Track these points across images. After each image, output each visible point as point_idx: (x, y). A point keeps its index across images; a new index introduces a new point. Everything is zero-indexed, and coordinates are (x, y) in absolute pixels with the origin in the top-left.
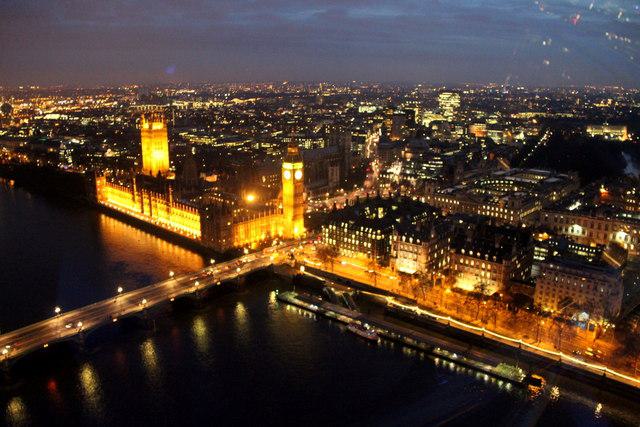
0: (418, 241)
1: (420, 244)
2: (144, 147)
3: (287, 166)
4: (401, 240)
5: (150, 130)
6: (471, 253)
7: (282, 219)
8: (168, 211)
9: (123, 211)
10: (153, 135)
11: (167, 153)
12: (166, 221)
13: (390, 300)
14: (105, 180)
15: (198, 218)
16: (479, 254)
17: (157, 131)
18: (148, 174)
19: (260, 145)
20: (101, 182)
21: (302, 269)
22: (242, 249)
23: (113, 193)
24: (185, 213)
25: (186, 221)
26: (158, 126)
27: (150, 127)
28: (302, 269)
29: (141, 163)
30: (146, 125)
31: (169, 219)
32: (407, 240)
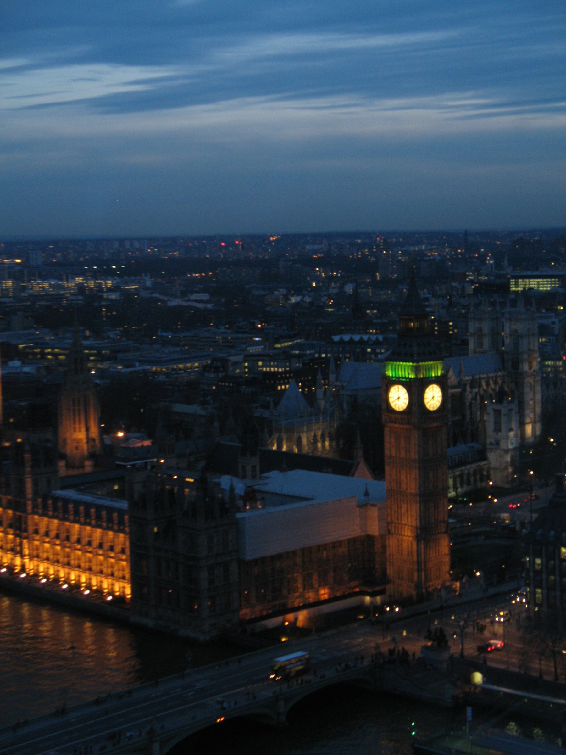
15: (122, 539)
21: (478, 677)
31: (17, 551)
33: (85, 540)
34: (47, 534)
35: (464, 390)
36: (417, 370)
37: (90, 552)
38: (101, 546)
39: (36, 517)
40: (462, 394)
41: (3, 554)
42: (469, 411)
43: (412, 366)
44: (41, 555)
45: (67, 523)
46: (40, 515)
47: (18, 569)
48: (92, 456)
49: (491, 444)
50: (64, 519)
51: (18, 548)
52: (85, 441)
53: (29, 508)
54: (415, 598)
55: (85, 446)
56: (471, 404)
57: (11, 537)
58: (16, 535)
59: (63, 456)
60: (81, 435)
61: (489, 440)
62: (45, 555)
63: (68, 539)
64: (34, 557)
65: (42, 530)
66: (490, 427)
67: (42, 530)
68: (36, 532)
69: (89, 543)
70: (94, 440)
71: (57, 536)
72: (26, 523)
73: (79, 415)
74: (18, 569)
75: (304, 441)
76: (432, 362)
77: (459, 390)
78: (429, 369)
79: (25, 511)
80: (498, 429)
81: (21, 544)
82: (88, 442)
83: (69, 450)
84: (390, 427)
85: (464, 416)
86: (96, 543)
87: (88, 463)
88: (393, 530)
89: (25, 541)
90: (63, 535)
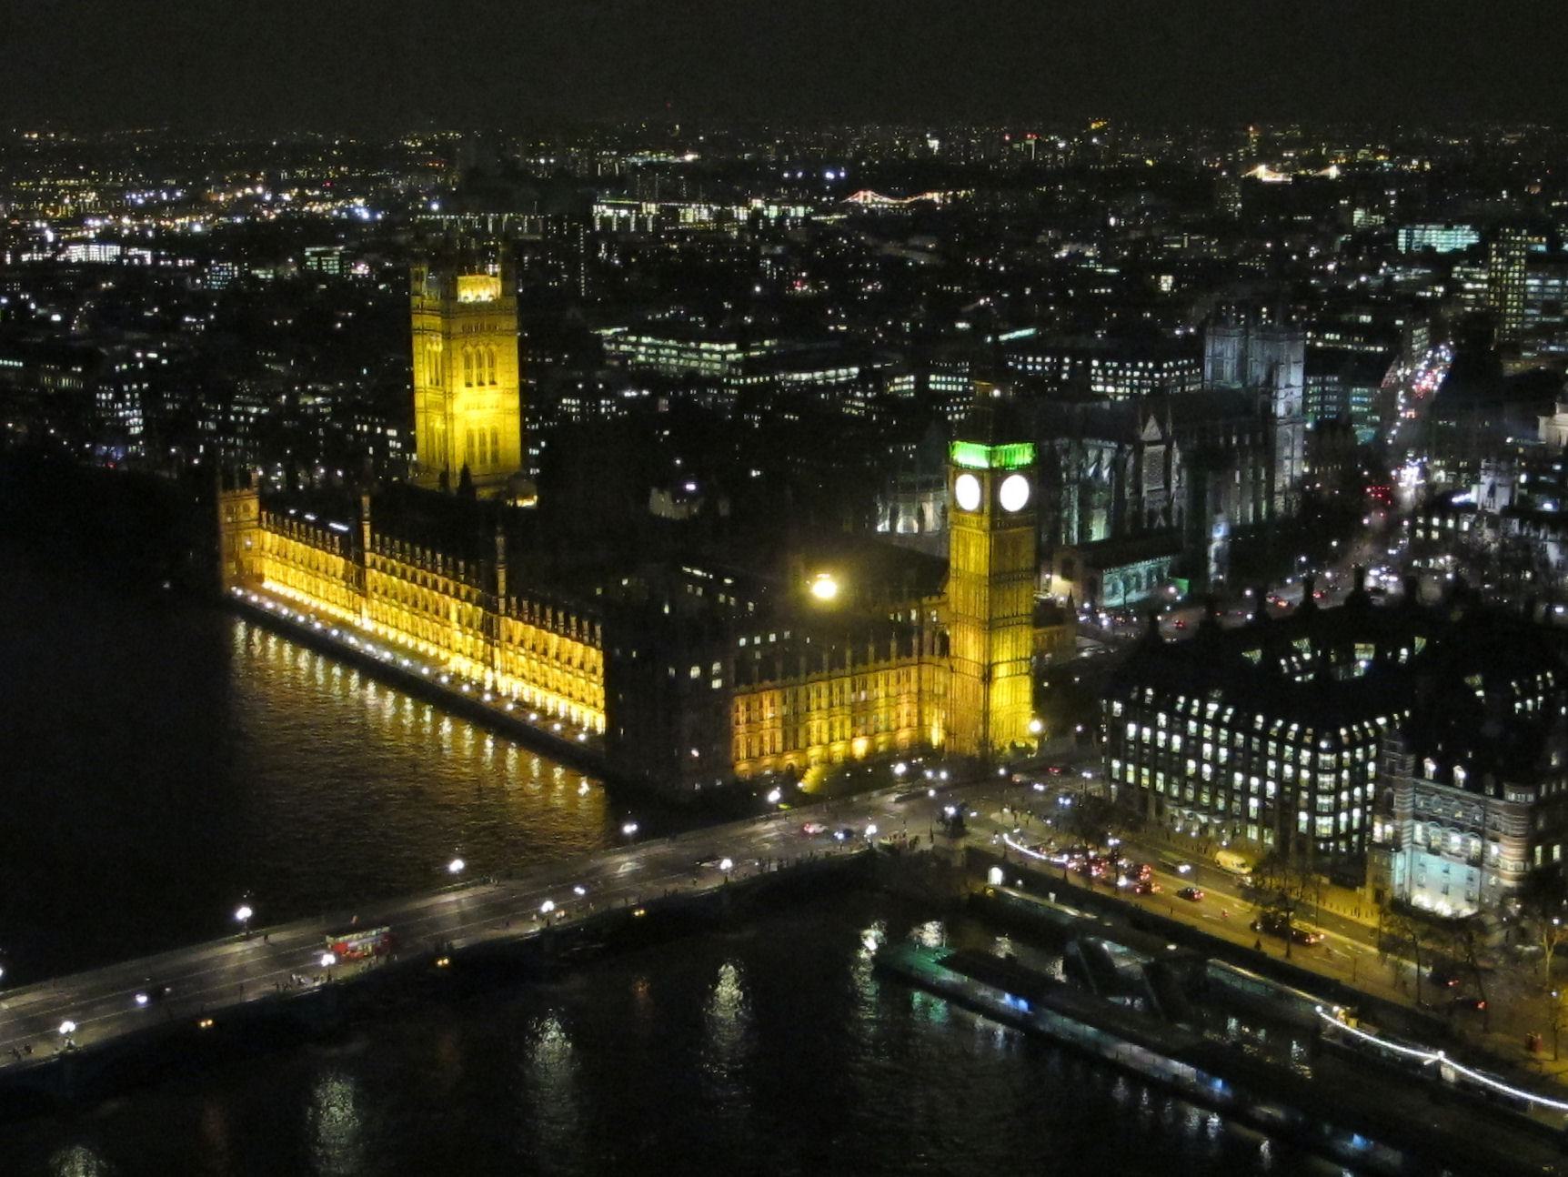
2: (423, 376)
3: (969, 454)
4: (1419, 771)
5: (450, 308)
7: (941, 677)
8: (489, 631)
10: (457, 328)
11: (514, 402)
12: (476, 671)
13: (1337, 1018)
14: (254, 505)
17: (478, 308)
18: (433, 484)
19: (921, 384)
21: (996, 876)
22: (762, 785)
23: (283, 556)
25: (555, 675)
28: (996, 876)
29: (410, 444)
32: (1445, 776)
33: (564, 657)
34: (522, 644)
35: (1169, 448)
36: (991, 456)
37: (570, 673)
38: (582, 666)
39: (510, 620)
40: (1168, 455)
41: (473, 665)
42: (1177, 478)
43: (986, 451)
44: (515, 670)
45: (544, 632)
46: (514, 619)
47: (488, 686)
50: (542, 627)
51: (489, 659)
53: (502, 606)
57: (481, 643)
58: (487, 641)
62: (519, 671)
63: (545, 653)
64: (507, 672)
65: (517, 639)
67: (517, 639)
68: (510, 640)
69: (569, 661)
71: (534, 648)
72: (498, 628)
74: (488, 686)
76: (1015, 445)
77: (1162, 448)
78: (1012, 454)
79: (495, 610)
81: (492, 655)
84: (958, 531)
86: (576, 662)
88: (956, 666)
89: (497, 651)
90: (540, 648)
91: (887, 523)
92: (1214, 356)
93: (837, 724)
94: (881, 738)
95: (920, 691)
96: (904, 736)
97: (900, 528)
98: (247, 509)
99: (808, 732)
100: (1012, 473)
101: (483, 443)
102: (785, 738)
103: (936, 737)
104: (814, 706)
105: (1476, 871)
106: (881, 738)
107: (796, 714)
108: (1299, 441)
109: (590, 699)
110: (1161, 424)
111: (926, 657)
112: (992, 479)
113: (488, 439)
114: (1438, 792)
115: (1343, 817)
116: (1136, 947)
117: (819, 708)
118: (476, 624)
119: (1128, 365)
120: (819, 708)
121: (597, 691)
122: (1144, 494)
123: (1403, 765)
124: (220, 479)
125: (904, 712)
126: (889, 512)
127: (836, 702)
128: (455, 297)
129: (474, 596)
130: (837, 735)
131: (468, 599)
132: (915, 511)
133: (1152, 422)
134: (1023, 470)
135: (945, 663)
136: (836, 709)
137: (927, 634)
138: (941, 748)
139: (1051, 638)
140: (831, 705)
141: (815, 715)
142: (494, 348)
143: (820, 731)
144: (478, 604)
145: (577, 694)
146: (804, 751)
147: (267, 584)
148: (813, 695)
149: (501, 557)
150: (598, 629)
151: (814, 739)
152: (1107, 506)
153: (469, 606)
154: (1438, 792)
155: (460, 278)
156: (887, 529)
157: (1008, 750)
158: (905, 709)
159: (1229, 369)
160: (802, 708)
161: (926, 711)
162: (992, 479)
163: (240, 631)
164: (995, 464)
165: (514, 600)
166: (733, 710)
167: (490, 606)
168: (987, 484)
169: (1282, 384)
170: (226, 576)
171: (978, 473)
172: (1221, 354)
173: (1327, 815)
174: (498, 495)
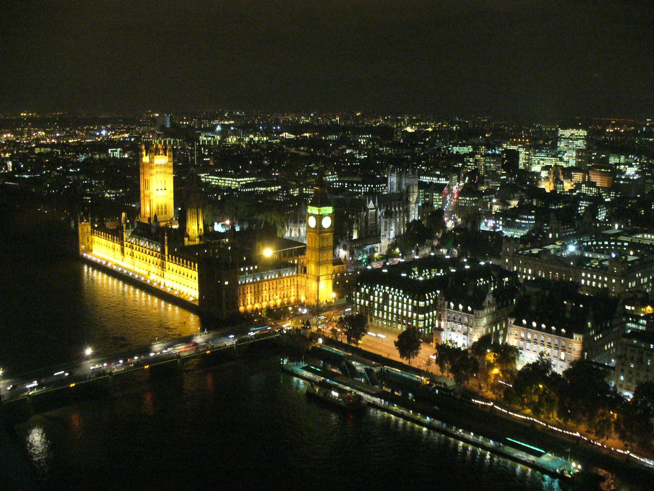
0: (470, 308)
1: (472, 313)
3: (312, 210)
4: (449, 306)
6: (534, 324)
7: (304, 280)
8: (163, 266)
9: (99, 261)
11: (172, 195)
12: (159, 279)
16: (543, 326)
18: (147, 222)
19: (301, 191)
20: (85, 227)
21: (320, 341)
24: (183, 269)
25: (184, 280)
26: (162, 160)
27: (151, 162)
28: (320, 341)
30: (146, 159)
32: (456, 308)
35: (377, 211)
36: (319, 210)
40: (376, 212)
47: (162, 284)
48: (200, 237)
49: (383, 236)
52: (197, 230)
54: (315, 306)
55: (197, 232)
56: (380, 217)
57: (160, 270)
59: (188, 236)
60: (195, 227)
61: (382, 234)
66: (383, 228)
70: (201, 230)
73: (195, 218)
75: (302, 231)
77: (375, 210)
79: (165, 260)
80: (386, 230)
82: (198, 230)
83: (190, 233)
85: (376, 222)
87: (197, 240)
91: (289, 233)
92: (391, 182)
93: (271, 295)
94: (286, 299)
95: (297, 284)
96: (292, 299)
97: (293, 236)
98: (87, 229)
99: (262, 297)
100: (325, 216)
101: (162, 208)
102: (255, 299)
103: (303, 299)
104: (264, 289)
105: (465, 336)
106: (286, 299)
107: (258, 291)
108: (417, 209)
109: (194, 288)
110: (374, 203)
111: (299, 274)
112: (319, 218)
113: (164, 207)
114: (454, 313)
115: (427, 321)
116: (363, 363)
117: (266, 290)
118: (159, 264)
119: (365, 186)
120: (266, 290)
121: (195, 284)
122: (369, 225)
123: (444, 304)
124: (79, 219)
125: (292, 292)
126: (289, 230)
127: (271, 288)
128: (153, 163)
129: (158, 255)
130: (271, 298)
131: (156, 256)
132: (297, 230)
133: (371, 202)
134: (329, 215)
135: (305, 275)
136: (271, 290)
137: (299, 267)
138: (304, 303)
139: (339, 269)
140: (269, 289)
141: (265, 292)
142: (165, 178)
143: (266, 296)
144: (159, 258)
145: (190, 286)
146: (261, 303)
147: (94, 252)
148: (264, 286)
149: (166, 243)
150: (196, 265)
151: (264, 300)
152: (357, 229)
153: (156, 258)
154: (454, 313)
155: (155, 157)
156: (289, 235)
157: (325, 303)
158: (293, 290)
159: (395, 187)
160: (260, 289)
161: (300, 290)
162: (319, 218)
163: (86, 267)
164: (320, 213)
165: (170, 256)
166: (238, 290)
167: (163, 259)
168: (318, 219)
169: (411, 191)
170: (81, 250)
171: (315, 216)
172: (393, 182)
173: (422, 321)
174: (167, 224)
